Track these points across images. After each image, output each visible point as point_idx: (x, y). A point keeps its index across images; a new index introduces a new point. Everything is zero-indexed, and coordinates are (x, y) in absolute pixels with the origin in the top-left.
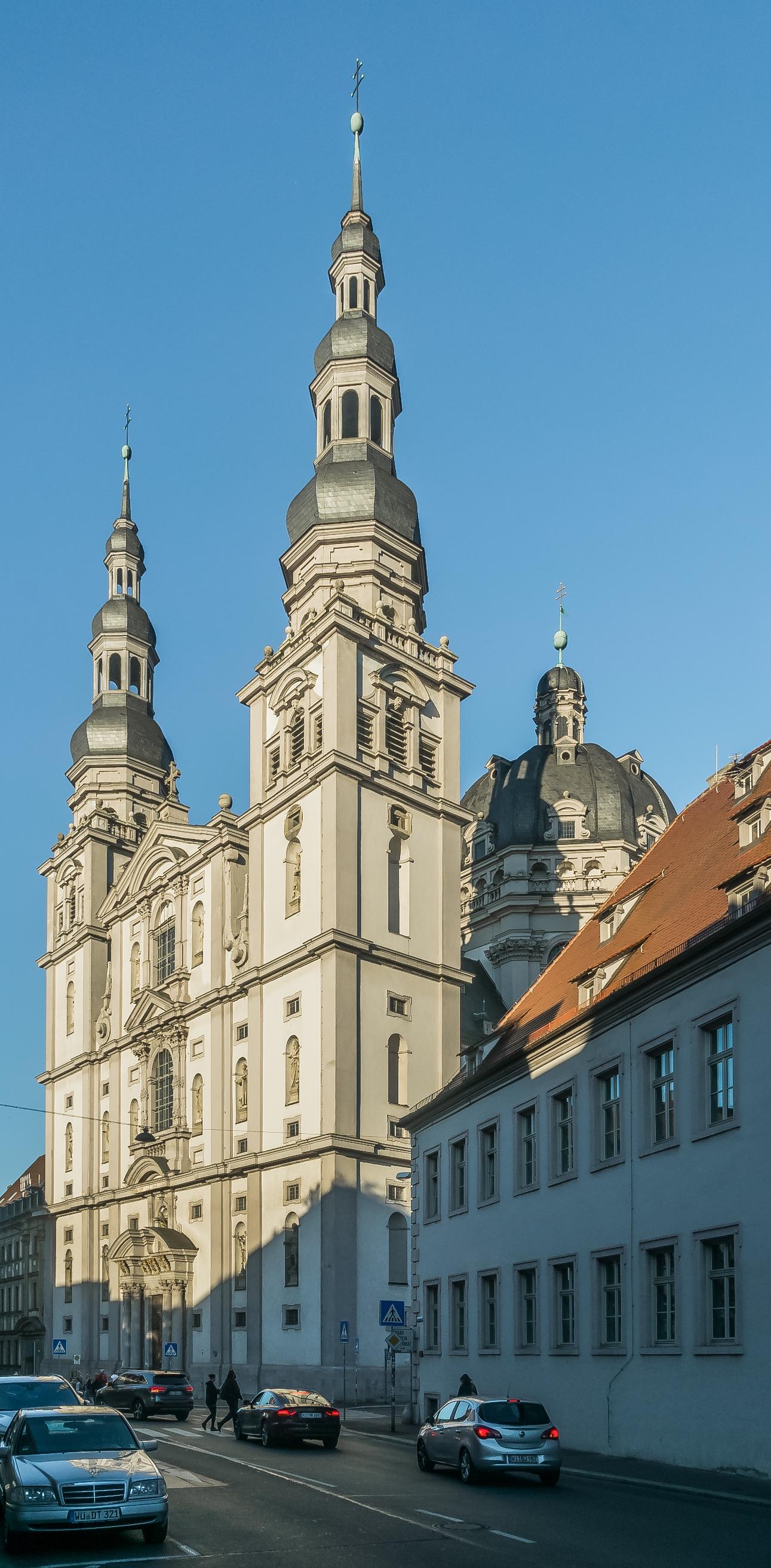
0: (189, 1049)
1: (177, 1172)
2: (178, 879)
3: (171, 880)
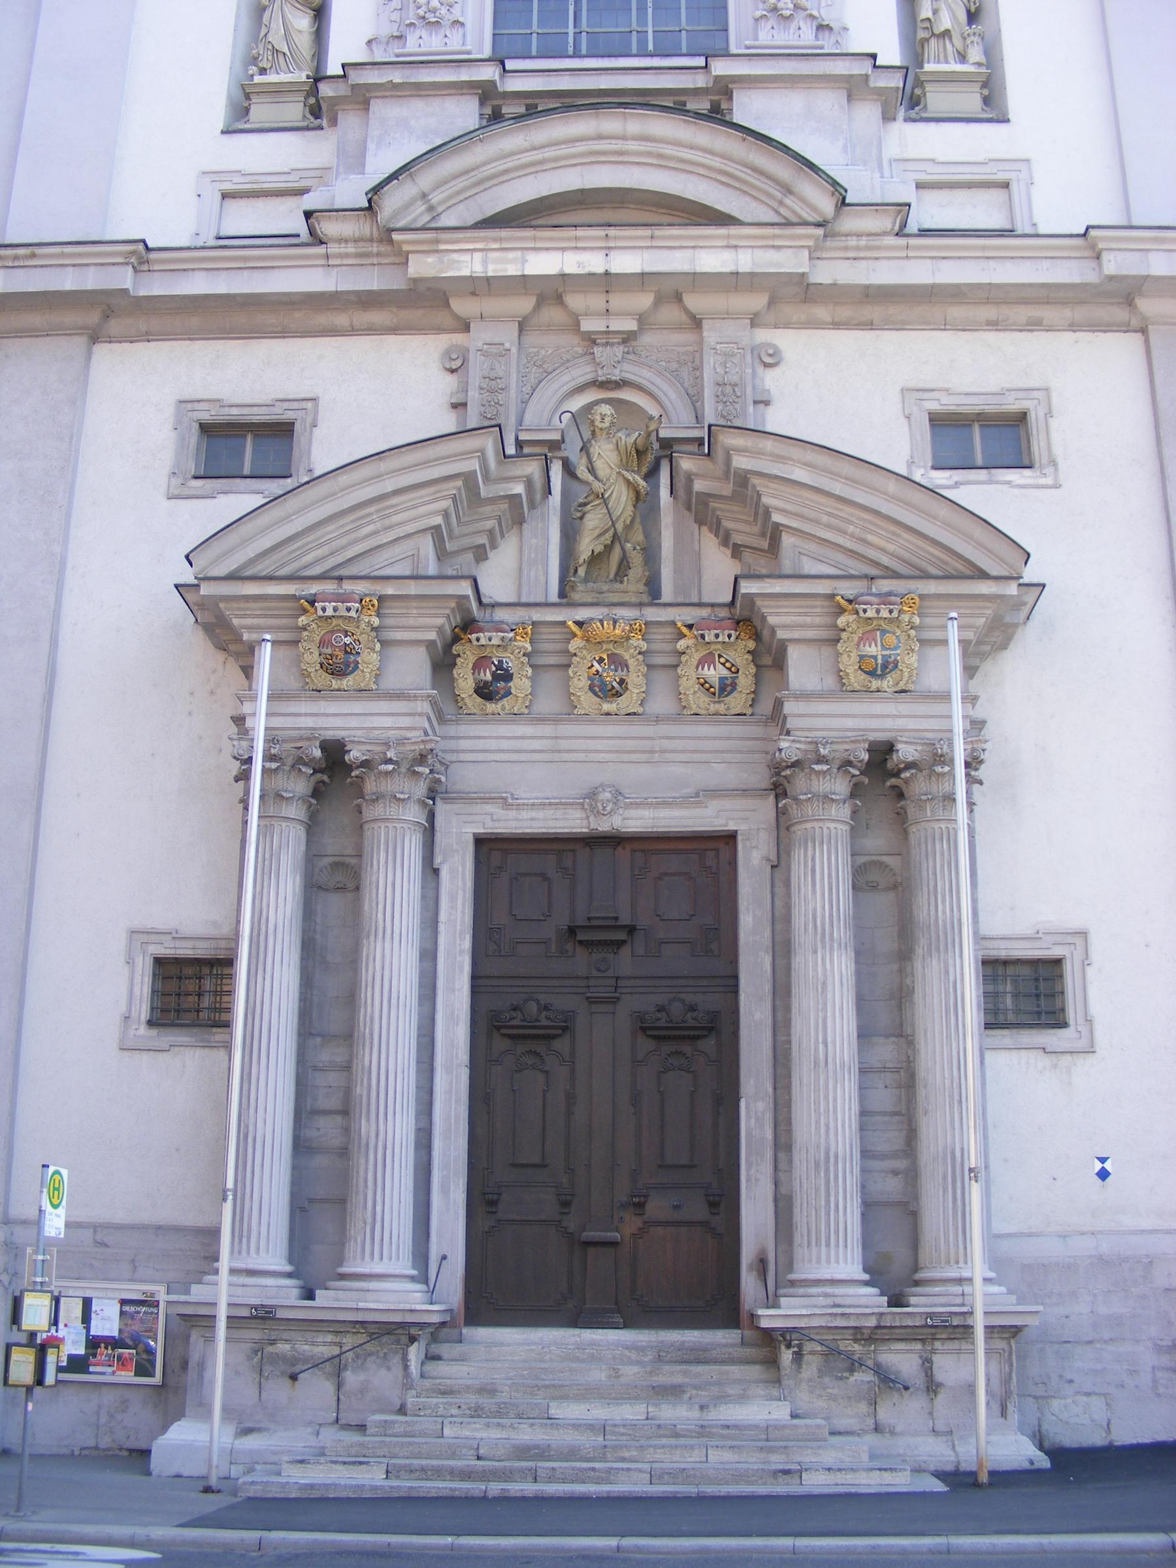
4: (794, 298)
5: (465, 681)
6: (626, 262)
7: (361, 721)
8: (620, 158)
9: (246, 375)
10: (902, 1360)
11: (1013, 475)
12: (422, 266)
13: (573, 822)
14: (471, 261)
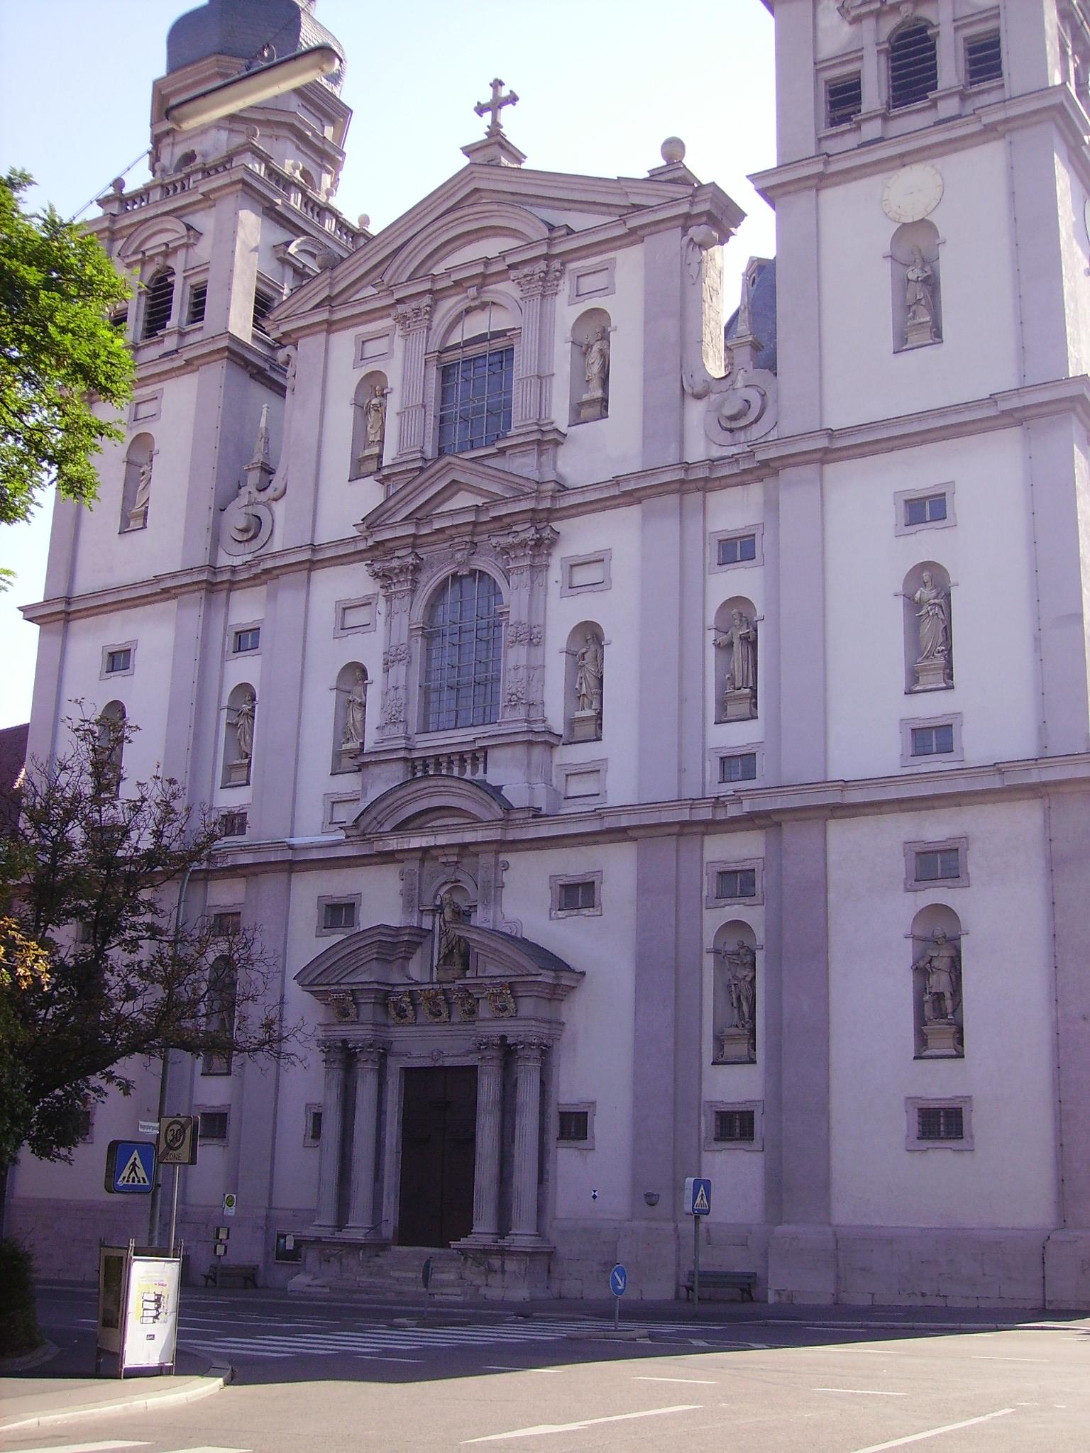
0: (555, 573)
1: (537, 814)
2: (542, 265)
3: (511, 267)
4: (505, 845)
5: (393, 1013)
6: (442, 840)
7: (358, 1033)
8: (440, 794)
9: (338, 884)
10: (496, 1262)
11: (585, 911)
12: (379, 846)
13: (428, 1063)
14: (393, 844)
